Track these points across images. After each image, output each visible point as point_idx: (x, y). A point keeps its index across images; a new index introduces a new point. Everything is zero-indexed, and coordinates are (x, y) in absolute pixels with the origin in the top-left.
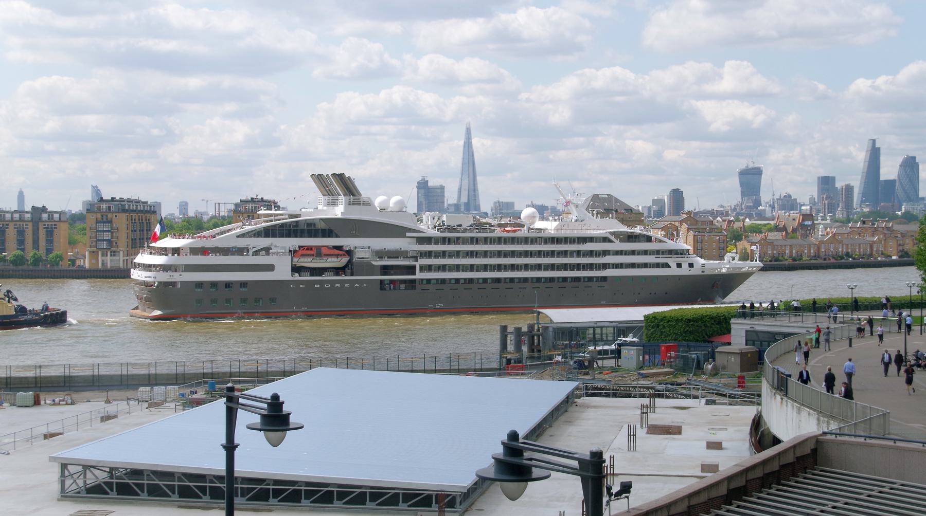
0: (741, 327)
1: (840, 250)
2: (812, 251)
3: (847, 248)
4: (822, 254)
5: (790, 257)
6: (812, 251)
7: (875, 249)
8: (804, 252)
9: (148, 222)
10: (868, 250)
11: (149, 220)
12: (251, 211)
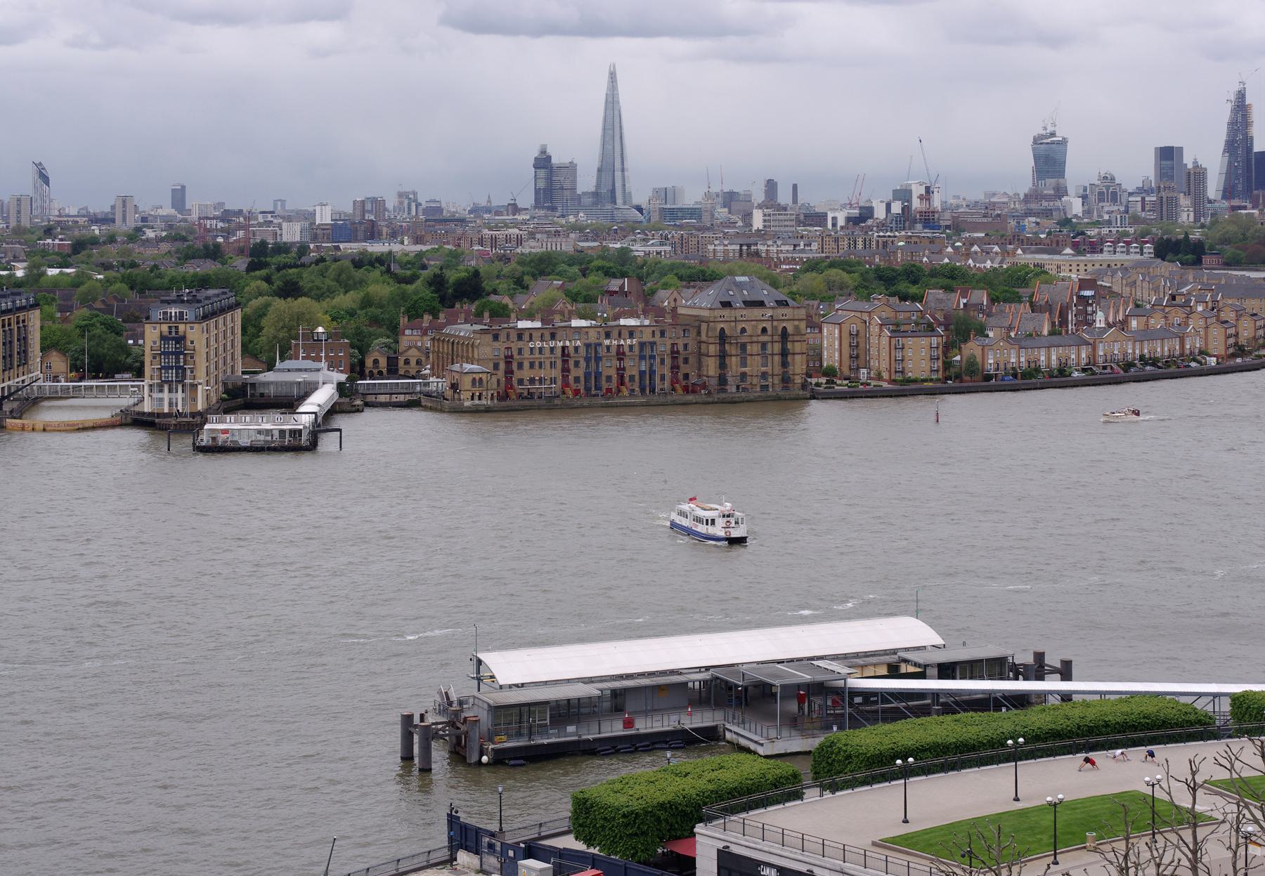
0: (710, 842)
1: (1130, 351)
2: (1084, 355)
3: (1142, 350)
4: (1100, 361)
5: (1048, 366)
6: (1084, 355)
7: (1188, 347)
8: (1070, 358)
9: (21, 325)
10: (1177, 348)
11: (24, 321)
12: (173, 319)
